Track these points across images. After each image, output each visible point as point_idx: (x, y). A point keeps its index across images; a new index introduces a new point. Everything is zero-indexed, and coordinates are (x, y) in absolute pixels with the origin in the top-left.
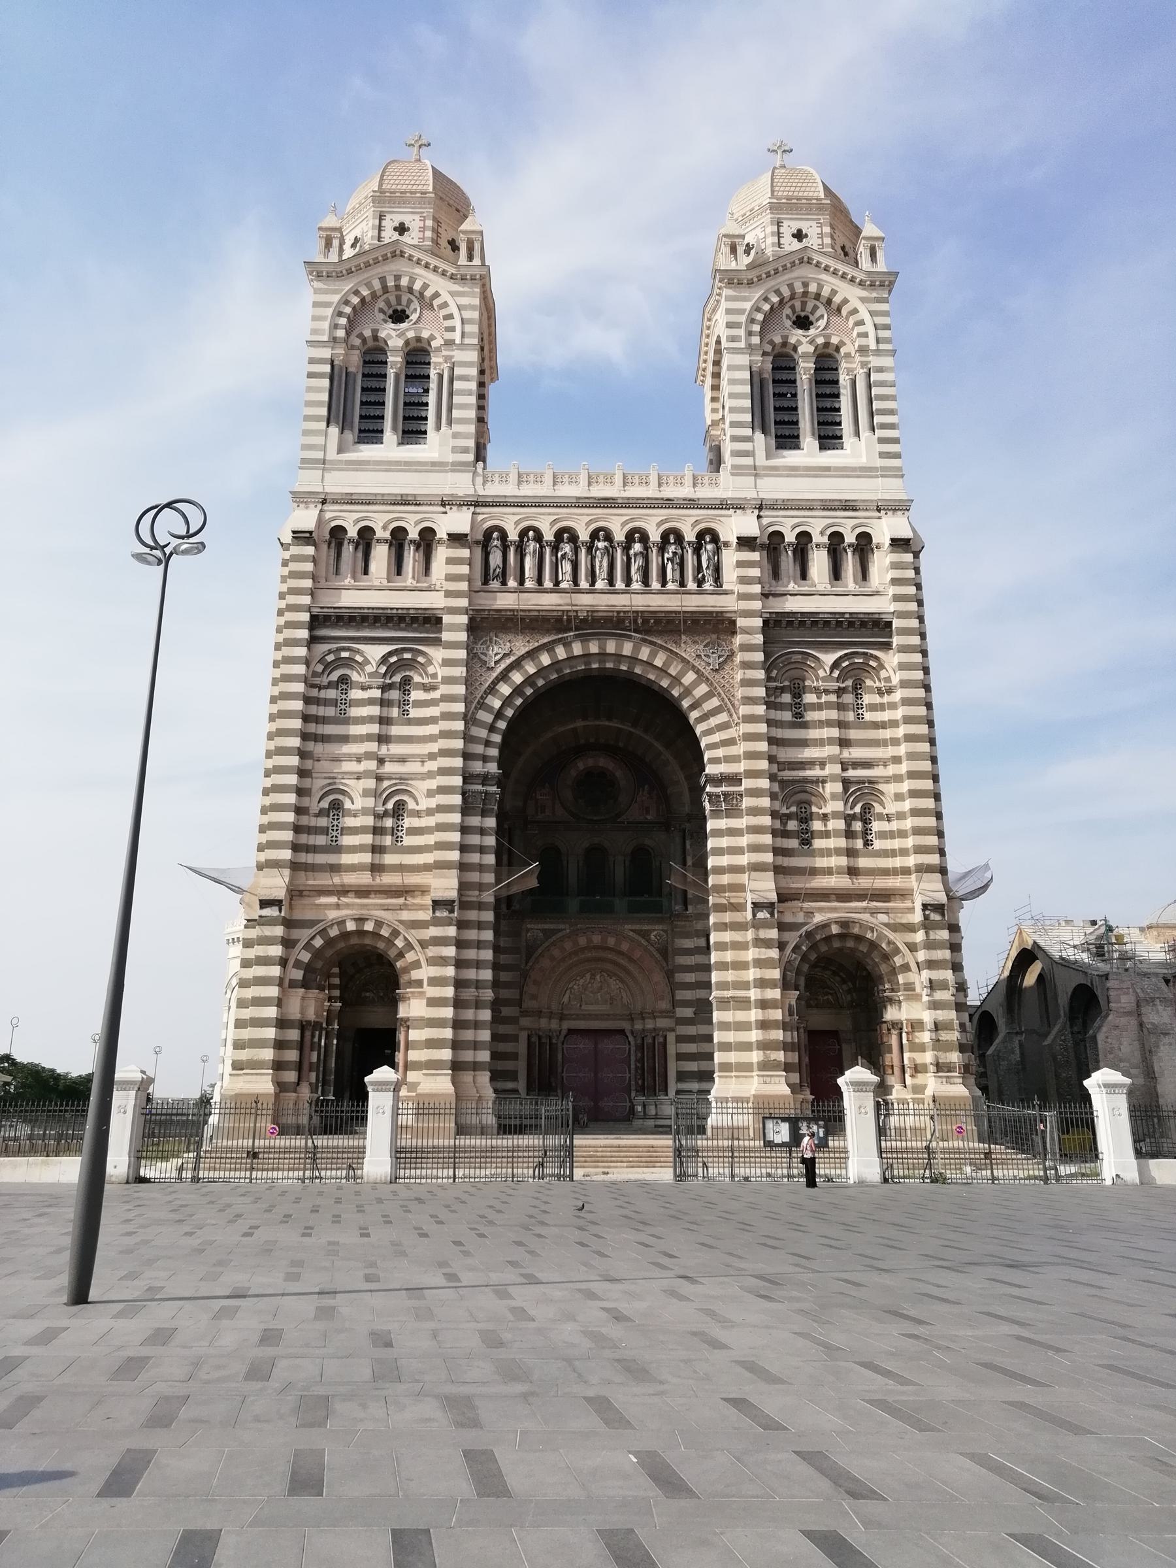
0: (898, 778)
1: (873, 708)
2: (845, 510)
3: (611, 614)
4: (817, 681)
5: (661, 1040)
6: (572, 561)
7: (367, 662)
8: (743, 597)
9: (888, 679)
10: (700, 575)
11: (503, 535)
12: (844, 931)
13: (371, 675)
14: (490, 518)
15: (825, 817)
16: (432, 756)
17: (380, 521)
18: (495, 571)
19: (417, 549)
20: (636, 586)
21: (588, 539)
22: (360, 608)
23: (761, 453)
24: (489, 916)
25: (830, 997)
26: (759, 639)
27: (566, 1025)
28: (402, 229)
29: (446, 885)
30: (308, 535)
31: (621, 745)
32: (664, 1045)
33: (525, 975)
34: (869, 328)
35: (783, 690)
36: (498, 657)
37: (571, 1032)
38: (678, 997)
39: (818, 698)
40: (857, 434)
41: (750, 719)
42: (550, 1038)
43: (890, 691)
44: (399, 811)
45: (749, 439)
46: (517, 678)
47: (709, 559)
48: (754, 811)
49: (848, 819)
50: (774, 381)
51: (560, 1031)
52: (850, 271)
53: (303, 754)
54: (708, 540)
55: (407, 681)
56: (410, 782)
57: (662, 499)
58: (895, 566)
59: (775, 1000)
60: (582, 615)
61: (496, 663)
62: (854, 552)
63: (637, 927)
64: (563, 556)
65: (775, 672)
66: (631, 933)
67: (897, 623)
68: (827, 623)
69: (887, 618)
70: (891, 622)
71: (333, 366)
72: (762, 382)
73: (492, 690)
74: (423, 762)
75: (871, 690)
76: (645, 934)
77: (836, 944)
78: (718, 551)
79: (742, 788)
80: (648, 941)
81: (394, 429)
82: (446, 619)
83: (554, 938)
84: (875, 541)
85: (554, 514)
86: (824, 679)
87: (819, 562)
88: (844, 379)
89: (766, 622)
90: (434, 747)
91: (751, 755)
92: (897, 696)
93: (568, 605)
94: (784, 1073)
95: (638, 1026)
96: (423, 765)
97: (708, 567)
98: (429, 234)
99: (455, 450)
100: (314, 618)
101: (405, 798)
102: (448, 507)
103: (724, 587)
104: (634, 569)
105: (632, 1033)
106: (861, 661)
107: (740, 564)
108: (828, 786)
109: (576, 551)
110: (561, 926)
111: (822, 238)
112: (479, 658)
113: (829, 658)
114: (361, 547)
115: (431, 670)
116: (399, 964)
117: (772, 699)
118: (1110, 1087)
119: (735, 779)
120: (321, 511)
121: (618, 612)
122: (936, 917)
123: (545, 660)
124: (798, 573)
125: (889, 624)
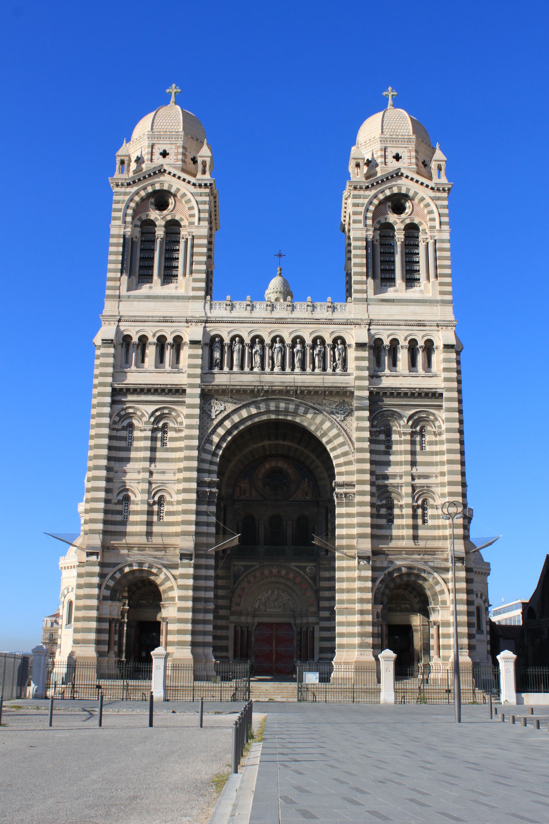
0: (442, 485)
1: (431, 443)
2: (419, 326)
3: (282, 388)
4: (400, 427)
5: (311, 629)
6: (260, 355)
7: (143, 415)
8: (358, 378)
9: (440, 427)
10: (335, 364)
11: (222, 340)
12: (410, 571)
13: (147, 423)
14: (214, 330)
15: (401, 507)
16: (180, 470)
18: (216, 361)
20: (297, 370)
21: (270, 342)
22: (140, 384)
23: (371, 291)
24: (212, 562)
25: (408, 606)
27: (257, 620)
28: (164, 154)
29: (189, 544)
30: (110, 342)
31: (291, 455)
32: (313, 632)
33: (233, 592)
34: (436, 215)
35: (380, 432)
36: (217, 412)
37: (259, 624)
38: (321, 605)
39: (400, 437)
40: (428, 278)
42: (248, 628)
43: (440, 434)
44: (160, 502)
46: (228, 424)
47: (340, 355)
48: (361, 504)
49: (415, 509)
50: (381, 244)
51: (254, 624)
52: (426, 181)
53: (108, 469)
54: (339, 343)
55: (165, 425)
56: (167, 485)
57: (313, 319)
58: (446, 360)
59: (368, 610)
60: (266, 388)
61: (216, 416)
62: (423, 351)
63: (298, 564)
65: (376, 422)
66: (295, 568)
67: (445, 395)
68: (406, 394)
69: (440, 391)
70: (442, 394)
72: (373, 246)
73: (214, 431)
74: (175, 473)
75: (430, 433)
76: (303, 568)
77: (405, 578)
78: (345, 349)
79: (354, 490)
80: (305, 572)
81: (159, 275)
82: (188, 391)
83: (250, 570)
84: (435, 345)
85: (250, 327)
86: (404, 427)
87: (403, 356)
88: (422, 246)
89: (371, 393)
90: (182, 465)
91: (360, 471)
92: (444, 437)
93: (258, 381)
94: (372, 650)
95: (298, 621)
96: (175, 475)
97: (339, 360)
98: (180, 157)
99: (194, 289)
100: (114, 390)
101: (165, 494)
102: (190, 323)
103: (349, 371)
104: (296, 360)
105: (295, 625)
106: (425, 416)
107: (357, 359)
108: (403, 488)
109: (263, 349)
110: (254, 563)
111: (410, 159)
112: (207, 413)
114: (140, 347)
115: (179, 420)
116: (161, 588)
117: (374, 438)
118: (506, 659)
119: (350, 485)
121: (286, 387)
122: (459, 564)
123: (244, 413)
124: (391, 362)
125: (441, 395)
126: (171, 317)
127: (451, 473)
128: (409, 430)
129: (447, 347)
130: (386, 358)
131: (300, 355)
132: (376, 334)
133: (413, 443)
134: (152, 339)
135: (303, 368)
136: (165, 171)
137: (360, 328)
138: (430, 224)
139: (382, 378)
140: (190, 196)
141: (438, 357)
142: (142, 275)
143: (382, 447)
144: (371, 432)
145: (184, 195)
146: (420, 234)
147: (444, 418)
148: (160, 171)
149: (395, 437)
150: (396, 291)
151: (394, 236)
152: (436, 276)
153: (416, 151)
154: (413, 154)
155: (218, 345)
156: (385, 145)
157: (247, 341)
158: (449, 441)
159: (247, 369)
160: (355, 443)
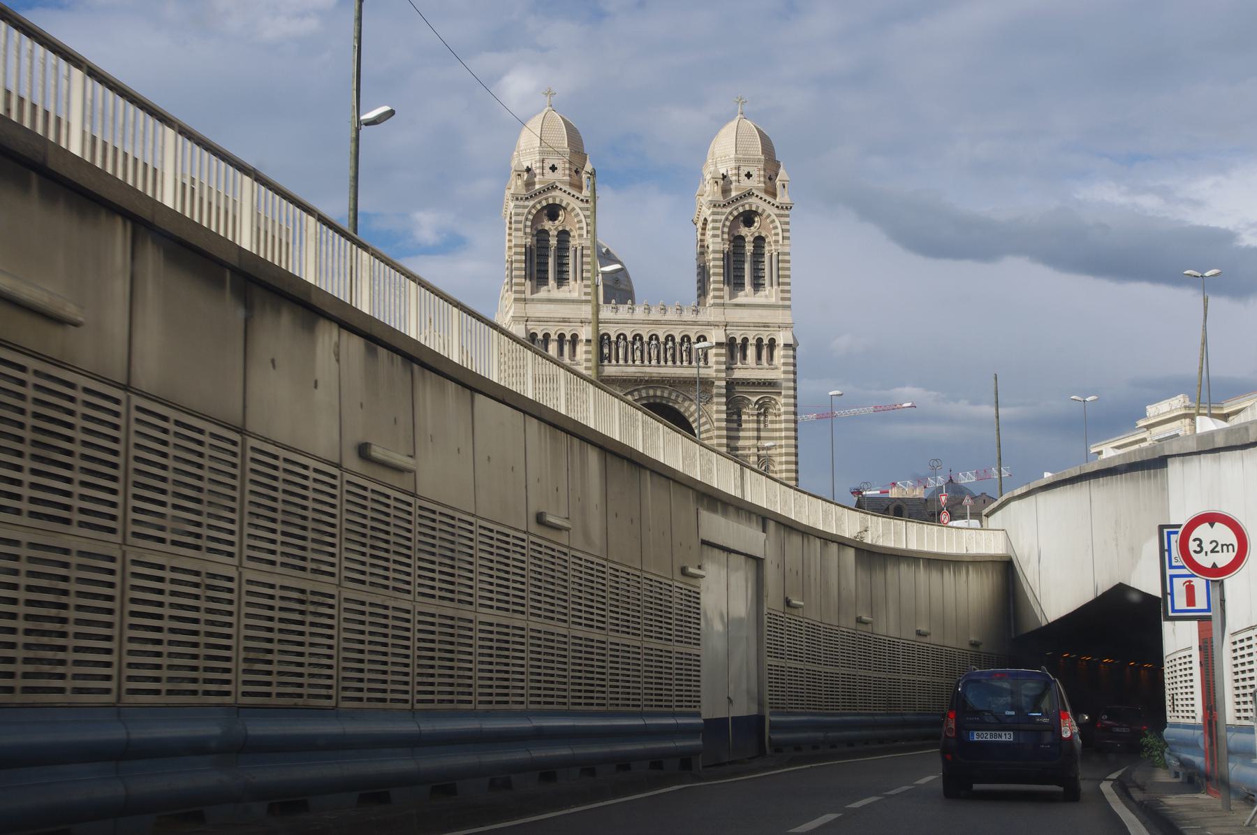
0: (781, 455)
1: (772, 422)
9: (779, 410)
11: (609, 337)
17: (554, 332)
19: (570, 344)
20: (670, 363)
23: (727, 297)
26: (724, 391)
28: (553, 168)
34: (779, 230)
35: (733, 414)
40: (772, 285)
41: (719, 428)
43: (779, 415)
45: (722, 290)
50: (734, 253)
58: (785, 356)
60: (646, 378)
64: (637, 348)
68: (754, 383)
71: (526, 247)
75: (771, 414)
84: (777, 343)
86: (752, 409)
87: (751, 352)
88: (767, 255)
89: (727, 382)
92: (783, 417)
99: (586, 294)
103: (709, 365)
107: (716, 355)
109: (642, 344)
113: (754, 399)
120: (526, 325)
126: (569, 318)
127: (787, 446)
128: (756, 412)
129: (786, 345)
130: (739, 354)
131: (671, 350)
132: (731, 334)
133: (758, 422)
134: (554, 337)
135: (674, 362)
136: (557, 187)
137: (719, 329)
138: (774, 238)
139: (735, 370)
140: (578, 210)
141: (779, 353)
142: (540, 278)
143: (735, 425)
144: (727, 413)
145: (573, 209)
146: (766, 245)
147: (783, 402)
148: (552, 187)
149: (744, 417)
150: (746, 296)
151: (744, 247)
152: (779, 284)
153: (765, 170)
154: (762, 173)
155: (607, 341)
156: (738, 164)
157: (630, 338)
158: (786, 421)
159: (630, 362)
160: (715, 423)
